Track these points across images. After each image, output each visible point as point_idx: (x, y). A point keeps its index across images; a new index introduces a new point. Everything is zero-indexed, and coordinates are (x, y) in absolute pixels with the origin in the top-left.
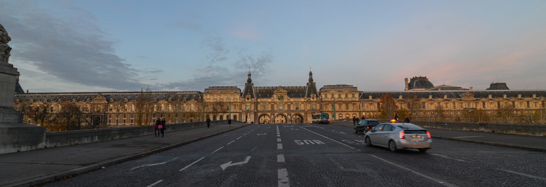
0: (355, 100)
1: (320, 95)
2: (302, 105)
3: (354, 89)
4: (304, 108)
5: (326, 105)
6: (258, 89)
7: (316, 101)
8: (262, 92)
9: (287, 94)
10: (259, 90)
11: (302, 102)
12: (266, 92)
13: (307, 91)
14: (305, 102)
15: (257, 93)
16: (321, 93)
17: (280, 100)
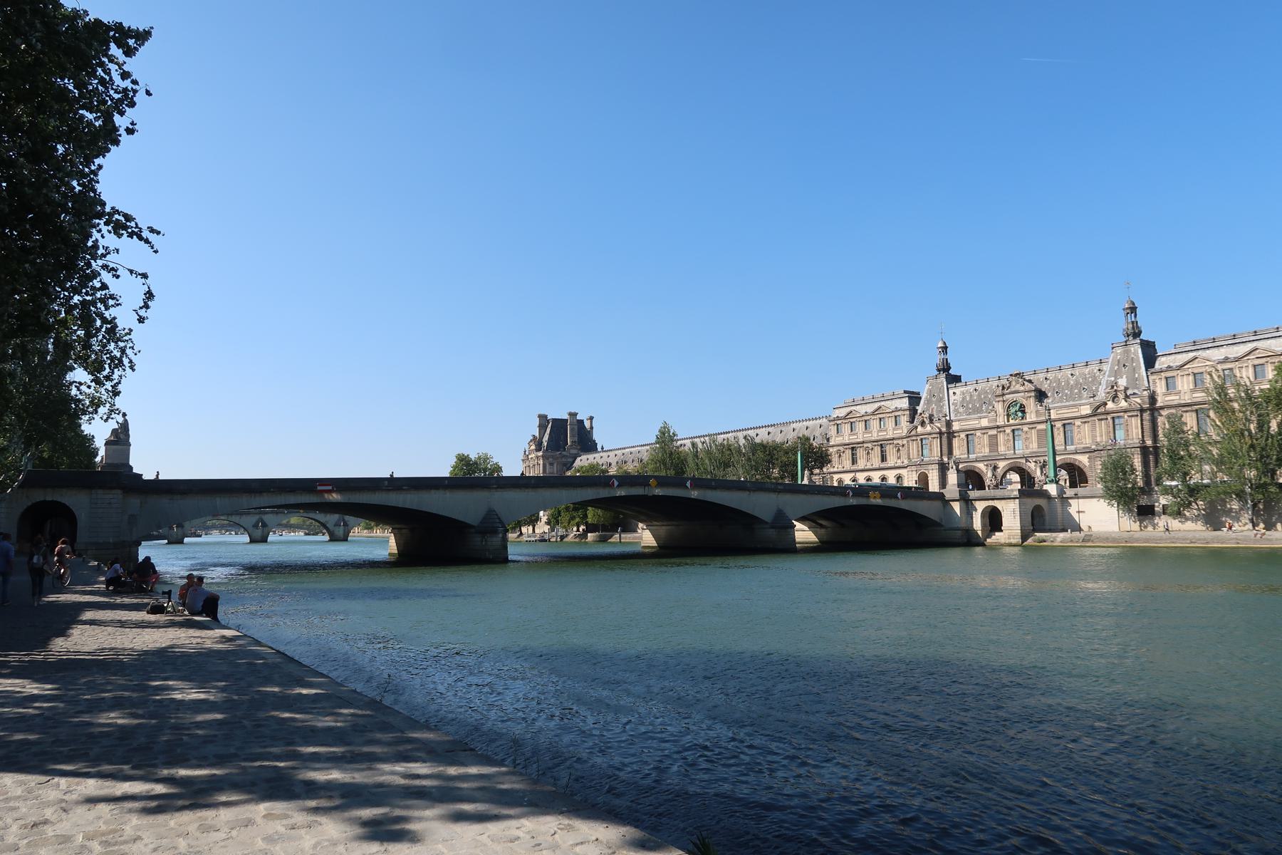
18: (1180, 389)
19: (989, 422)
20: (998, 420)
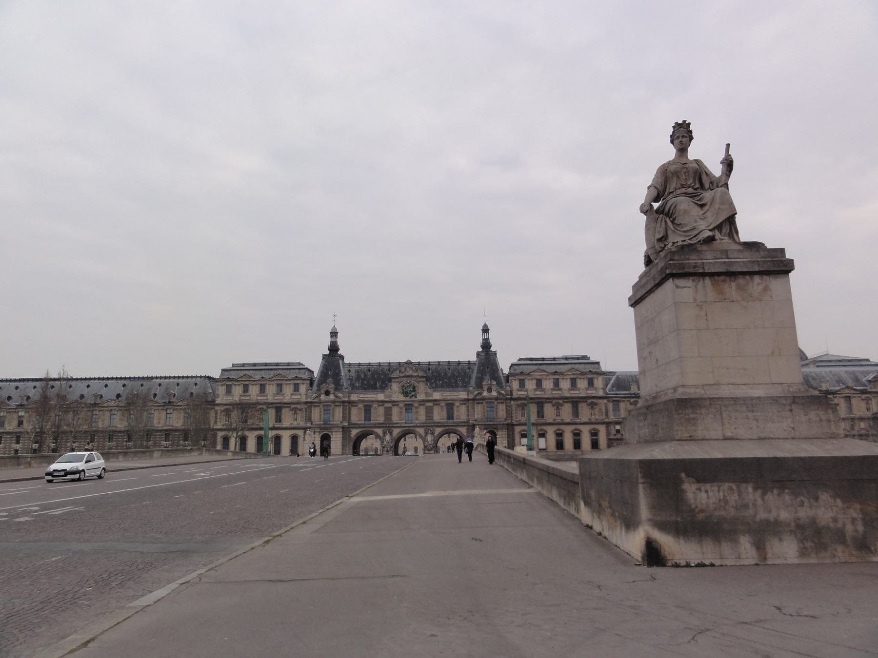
0: (594, 395)
1: (507, 381)
2: (463, 409)
3: (592, 366)
4: (468, 415)
5: (523, 407)
6: (353, 370)
7: (496, 399)
8: (363, 376)
9: (424, 379)
10: (357, 371)
11: (462, 400)
12: (373, 375)
13: (475, 371)
14: (468, 400)
15: (350, 379)
16: (510, 378)
17: (407, 396)
18: (527, 388)
19: (385, 396)
20: (393, 396)
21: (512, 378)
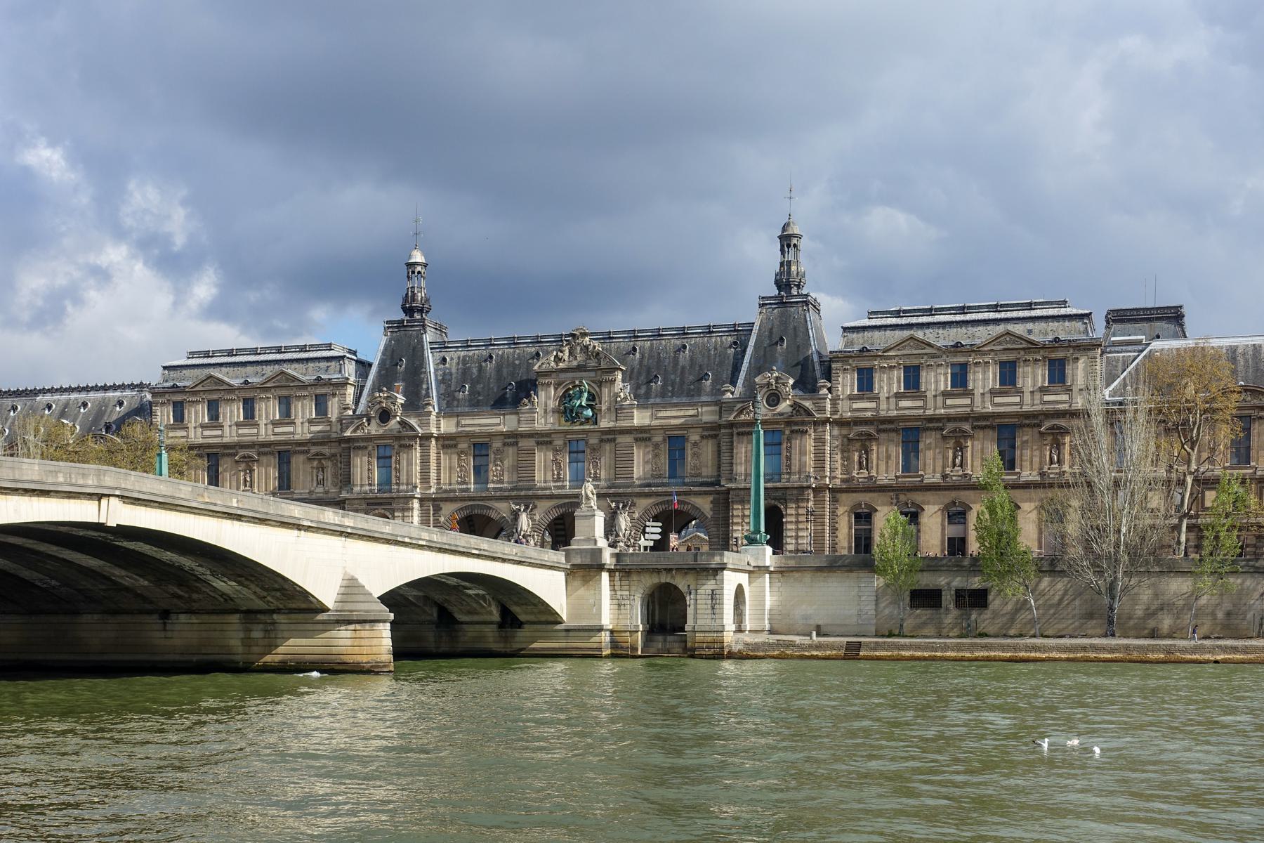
1: (828, 375)
10: (464, 361)
21: (839, 365)
